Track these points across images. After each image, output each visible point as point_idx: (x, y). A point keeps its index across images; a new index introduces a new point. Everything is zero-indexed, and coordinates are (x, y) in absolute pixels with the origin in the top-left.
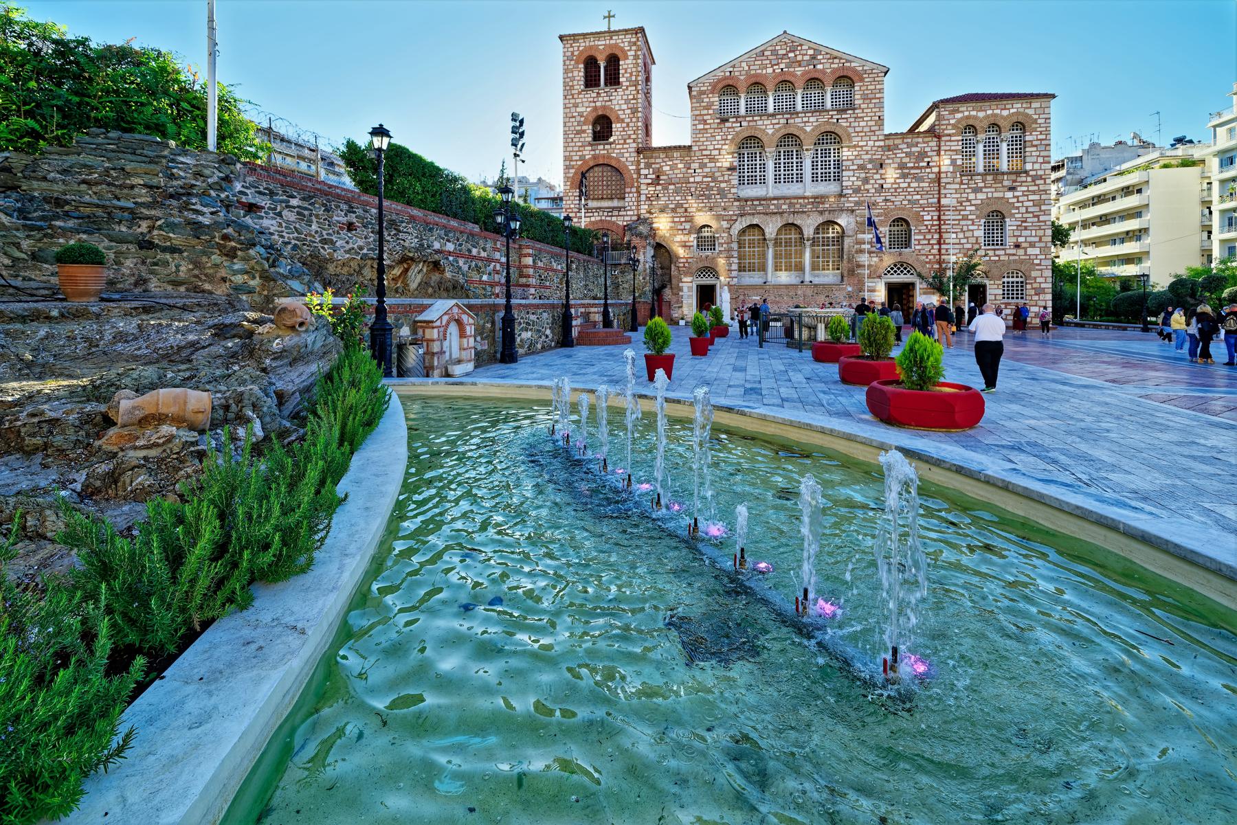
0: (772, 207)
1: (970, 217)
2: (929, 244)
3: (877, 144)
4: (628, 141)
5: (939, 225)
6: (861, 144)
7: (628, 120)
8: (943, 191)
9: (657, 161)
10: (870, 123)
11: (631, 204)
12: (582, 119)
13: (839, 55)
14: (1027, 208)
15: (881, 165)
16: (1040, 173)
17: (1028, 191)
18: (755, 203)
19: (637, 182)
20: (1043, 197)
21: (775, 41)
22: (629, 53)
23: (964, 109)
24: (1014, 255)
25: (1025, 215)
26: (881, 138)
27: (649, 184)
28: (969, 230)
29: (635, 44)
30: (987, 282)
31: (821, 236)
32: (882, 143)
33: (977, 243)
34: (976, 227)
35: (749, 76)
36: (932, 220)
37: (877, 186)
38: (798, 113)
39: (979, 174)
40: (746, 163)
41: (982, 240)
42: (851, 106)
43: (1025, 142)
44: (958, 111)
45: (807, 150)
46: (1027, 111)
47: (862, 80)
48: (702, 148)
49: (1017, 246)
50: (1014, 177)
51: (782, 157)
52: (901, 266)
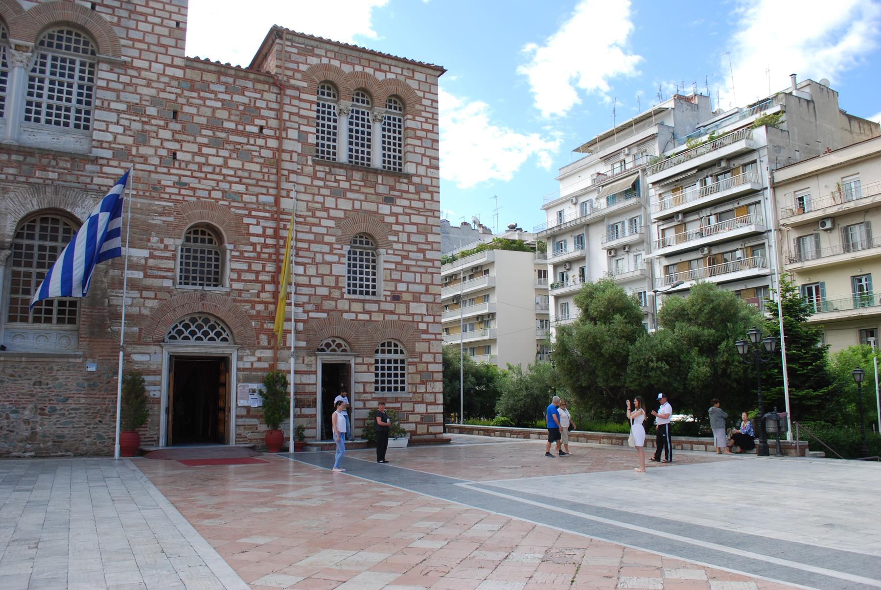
1: (327, 239)
2: (257, 281)
3: (170, 71)
5: (277, 247)
6: (137, 63)
8: (285, 185)
10: (158, 29)
14: (409, 234)
15: (175, 113)
16: (426, 181)
17: (411, 208)
20: (431, 221)
23: (323, 52)
24: (391, 313)
25: (407, 247)
26: (178, 62)
28: (325, 262)
31: (36, 243)
32: (179, 73)
34: (335, 258)
36: (264, 235)
39: (341, 166)
41: (344, 282)
43: (406, 129)
45: (18, 48)
46: (409, 82)
49: (396, 298)
50: (391, 181)
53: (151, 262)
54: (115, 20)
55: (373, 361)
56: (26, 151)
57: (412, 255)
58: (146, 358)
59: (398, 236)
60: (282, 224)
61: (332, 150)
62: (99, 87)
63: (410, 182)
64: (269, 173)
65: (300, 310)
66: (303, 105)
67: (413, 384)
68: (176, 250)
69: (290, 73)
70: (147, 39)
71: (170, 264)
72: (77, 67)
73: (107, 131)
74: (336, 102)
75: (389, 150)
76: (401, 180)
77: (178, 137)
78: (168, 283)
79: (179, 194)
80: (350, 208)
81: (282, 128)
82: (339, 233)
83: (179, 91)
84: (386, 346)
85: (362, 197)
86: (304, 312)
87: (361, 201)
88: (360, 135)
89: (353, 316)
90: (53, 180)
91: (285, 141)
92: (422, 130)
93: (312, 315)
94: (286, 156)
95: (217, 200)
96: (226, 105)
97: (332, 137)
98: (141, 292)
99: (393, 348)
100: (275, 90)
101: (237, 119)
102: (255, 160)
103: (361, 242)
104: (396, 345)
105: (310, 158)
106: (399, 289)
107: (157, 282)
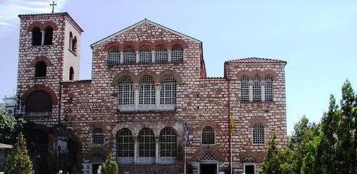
2: (224, 142)
3: (196, 83)
5: (229, 131)
13: (174, 33)
26: (198, 80)
27: (65, 103)
29: (62, 21)
31: (166, 135)
35: (125, 42)
40: (123, 92)
42: (182, 61)
44: (238, 67)
52: (209, 154)
56: (161, 112)
63: (275, 104)
71: (199, 139)
94: (231, 103)
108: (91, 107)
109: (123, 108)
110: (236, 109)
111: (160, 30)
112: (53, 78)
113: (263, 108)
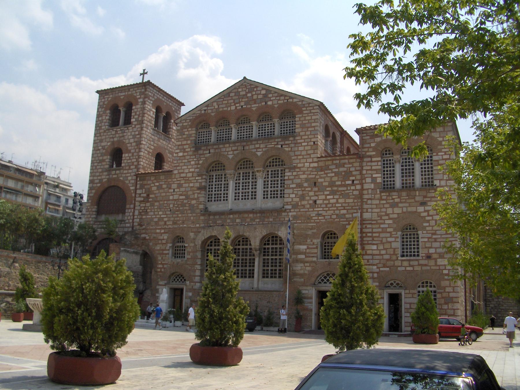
0: (228, 221)
1: (388, 230)
3: (312, 165)
4: (132, 167)
6: (299, 165)
7: (133, 151)
8: (365, 206)
9: (149, 182)
10: (307, 148)
11: (129, 218)
12: (104, 151)
13: (284, 93)
15: (315, 183)
18: (217, 217)
19: (135, 200)
21: (237, 86)
22: (140, 100)
24: (426, 265)
26: (315, 160)
27: (141, 202)
29: (143, 93)
30: (403, 292)
31: (270, 246)
32: (315, 165)
33: (394, 254)
34: (393, 239)
37: (311, 202)
38: (251, 141)
40: (214, 183)
41: (399, 252)
42: (293, 133)
45: (258, 171)
47: (301, 112)
48: (181, 171)
49: (429, 257)
50: (424, 193)
51: (241, 178)
53: (308, 251)
54: (290, 149)
55: (415, 291)
56: (262, 212)
57: (438, 232)
58: (307, 292)
59: (429, 223)
60: (364, 226)
61: (392, 183)
62: (287, 180)
64: (357, 202)
65: (375, 267)
66: (373, 164)
67: (439, 304)
68: (318, 244)
69: (366, 150)
70: (302, 154)
71: (315, 251)
72: (280, 172)
73: (289, 197)
74: (392, 157)
75: (425, 175)
76: (430, 191)
77: (317, 194)
78: (315, 259)
79: (318, 219)
80: (400, 212)
81: (363, 178)
82: (395, 226)
83: (316, 173)
84: (425, 284)
85: (407, 205)
86: (377, 268)
87: (406, 207)
88: (408, 171)
89: (403, 269)
90: (271, 221)
91: (364, 185)
92: (443, 159)
93: (381, 269)
94: (365, 192)
95: (334, 219)
96: (336, 174)
97: (392, 176)
98: (304, 264)
99: (429, 285)
100: (358, 160)
101: (342, 179)
102: (351, 197)
103: (410, 229)
104: (431, 283)
105: (378, 190)
106: (430, 252)
107: (310, 259)
108: (171, 206)
109: (214, 207)
110: (375, 202)
111: (263, 92)
112: (130, 169)
113: (417, 199)
